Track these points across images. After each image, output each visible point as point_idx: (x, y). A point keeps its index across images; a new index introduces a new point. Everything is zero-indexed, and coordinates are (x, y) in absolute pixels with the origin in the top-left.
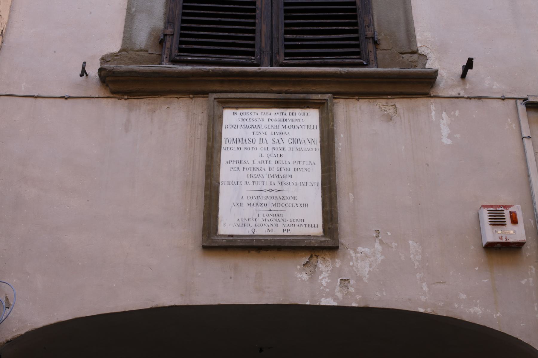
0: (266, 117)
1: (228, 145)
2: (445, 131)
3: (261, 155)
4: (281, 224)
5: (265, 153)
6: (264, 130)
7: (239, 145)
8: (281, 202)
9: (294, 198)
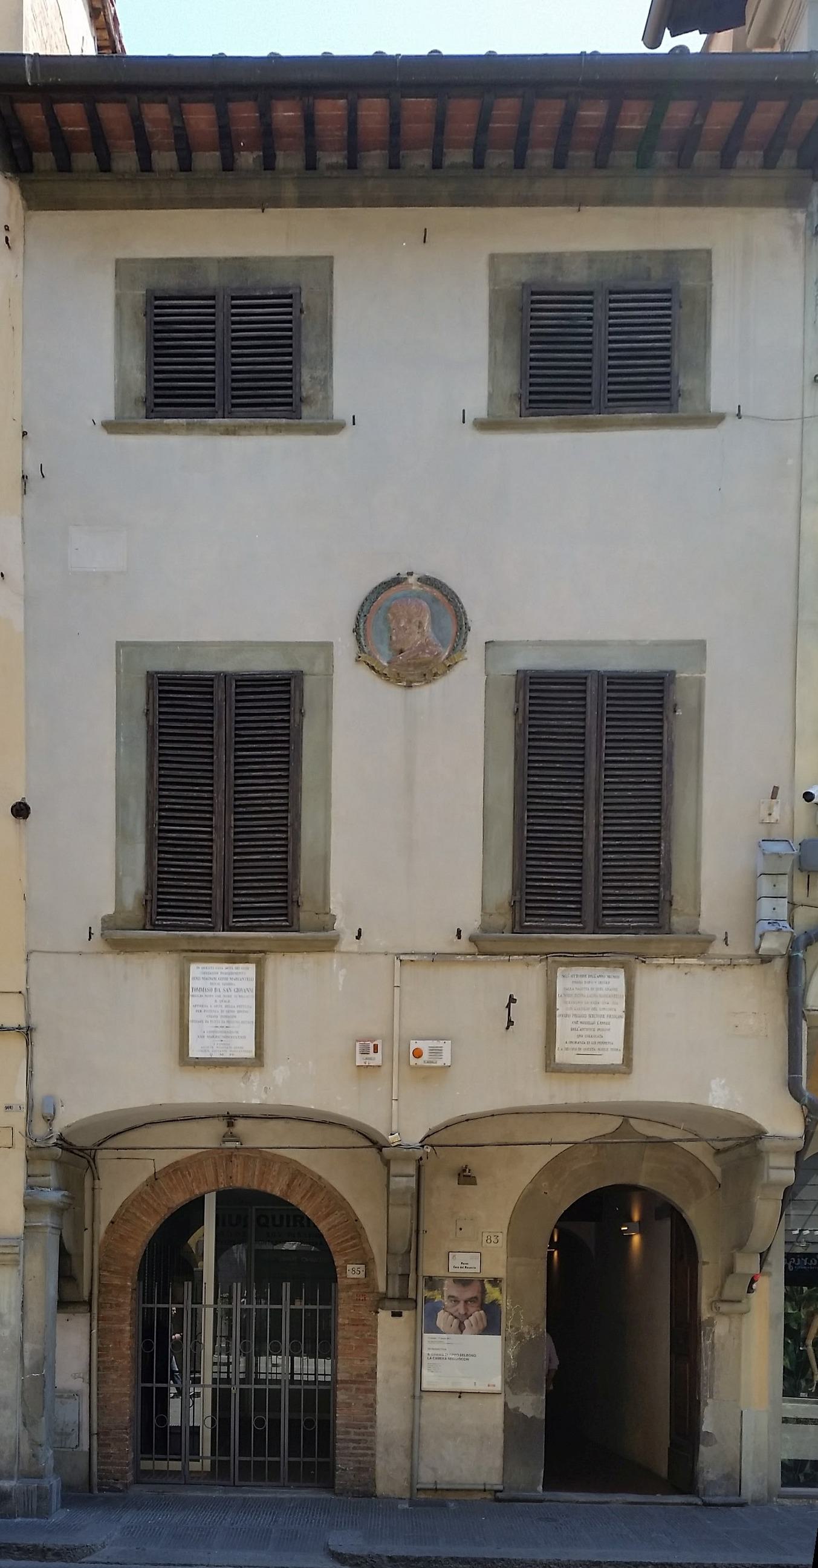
0: (219, 971)
1: (194, 993)
2: (341, 980)
3: (216, 1001)
4: (228, 1050)
5: (218, 999)
6: (218, 981)
7: (202, 993)
8: (229, 1035)
9: (237, 1032)
